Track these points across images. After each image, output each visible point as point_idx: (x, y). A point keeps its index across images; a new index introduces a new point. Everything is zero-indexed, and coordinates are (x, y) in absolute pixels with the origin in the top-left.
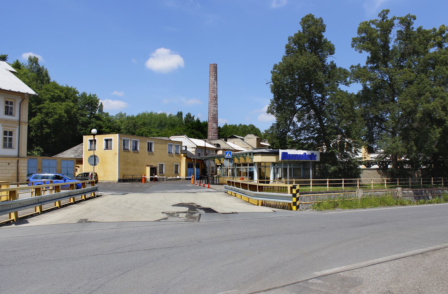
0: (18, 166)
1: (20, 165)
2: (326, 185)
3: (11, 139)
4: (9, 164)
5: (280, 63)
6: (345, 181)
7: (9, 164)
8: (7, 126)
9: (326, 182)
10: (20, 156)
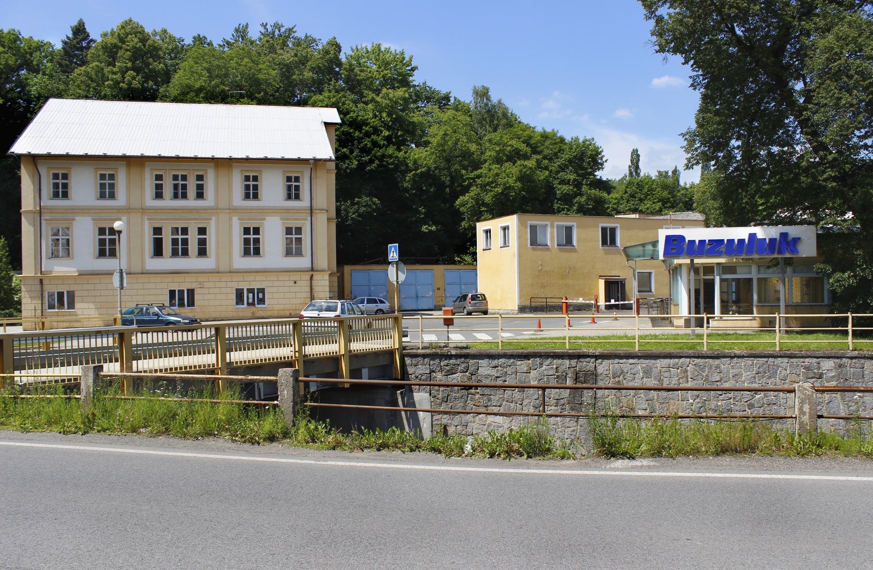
0: (311, 286)
1: (314, 283)
2: (846, 333)
3: (299, 240)
4: (295, 283)
5: (310, 41)
6: (857, 322)
7: (295, 283)
8: (288, 219)
9: (844, 322)
10: (315, 268)
